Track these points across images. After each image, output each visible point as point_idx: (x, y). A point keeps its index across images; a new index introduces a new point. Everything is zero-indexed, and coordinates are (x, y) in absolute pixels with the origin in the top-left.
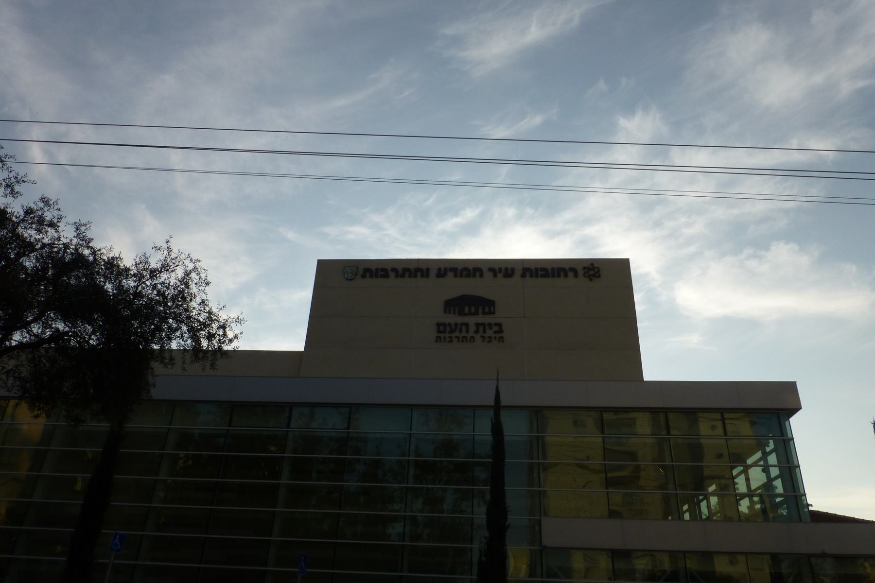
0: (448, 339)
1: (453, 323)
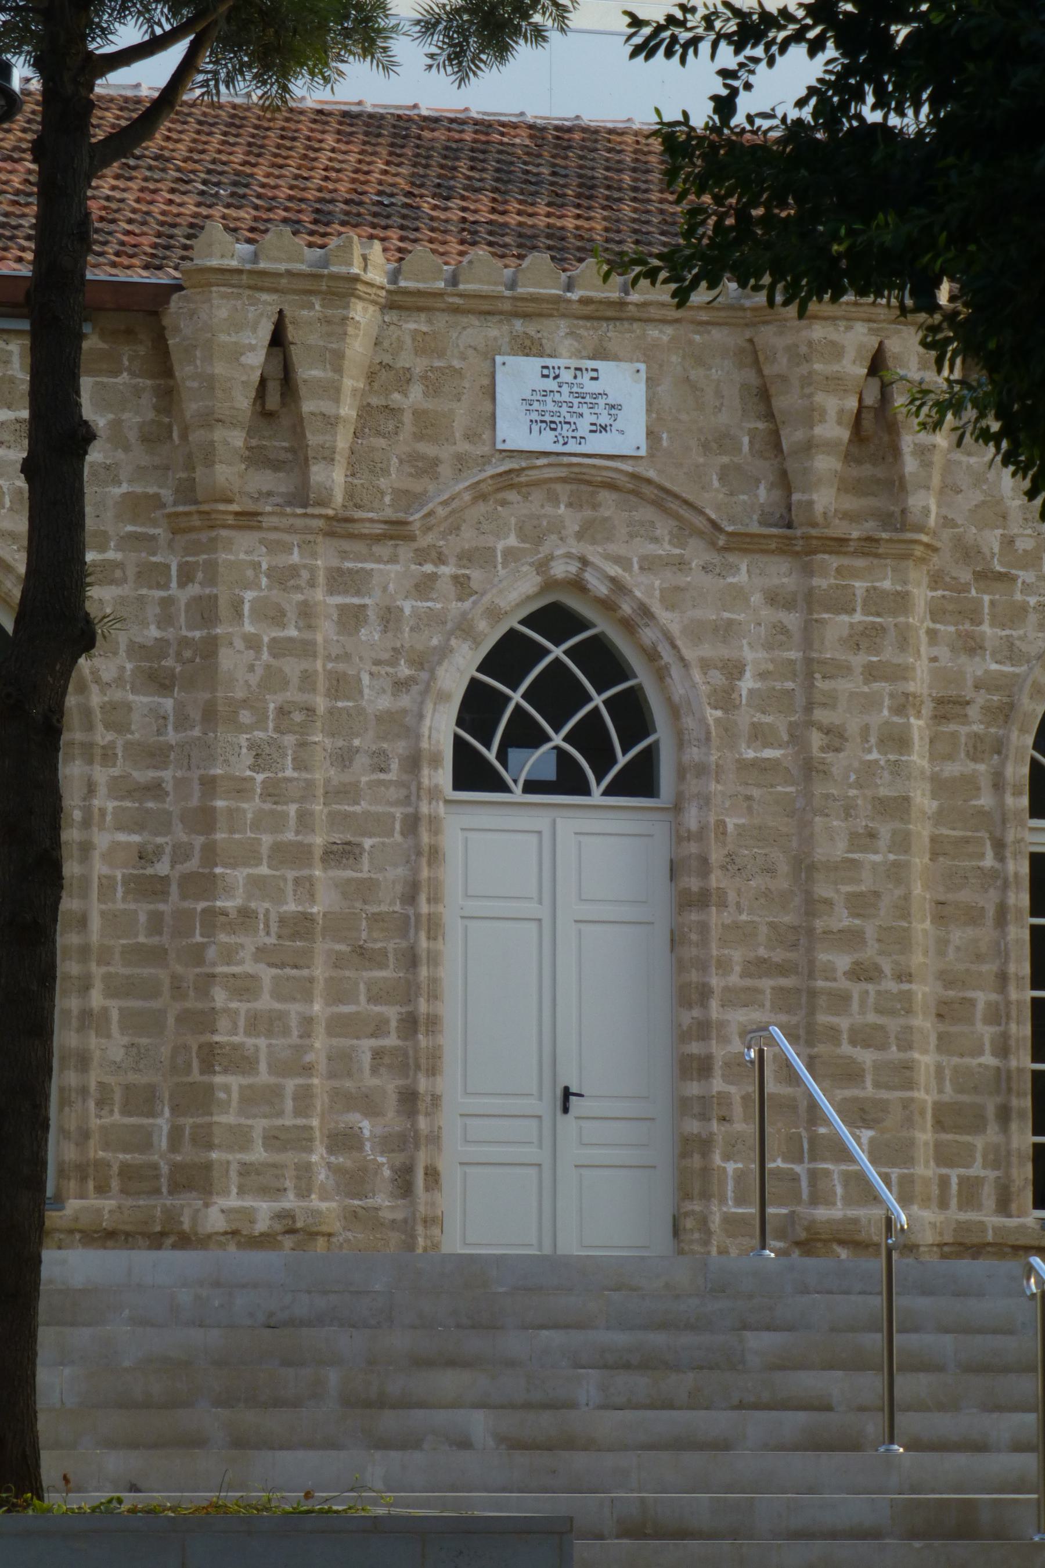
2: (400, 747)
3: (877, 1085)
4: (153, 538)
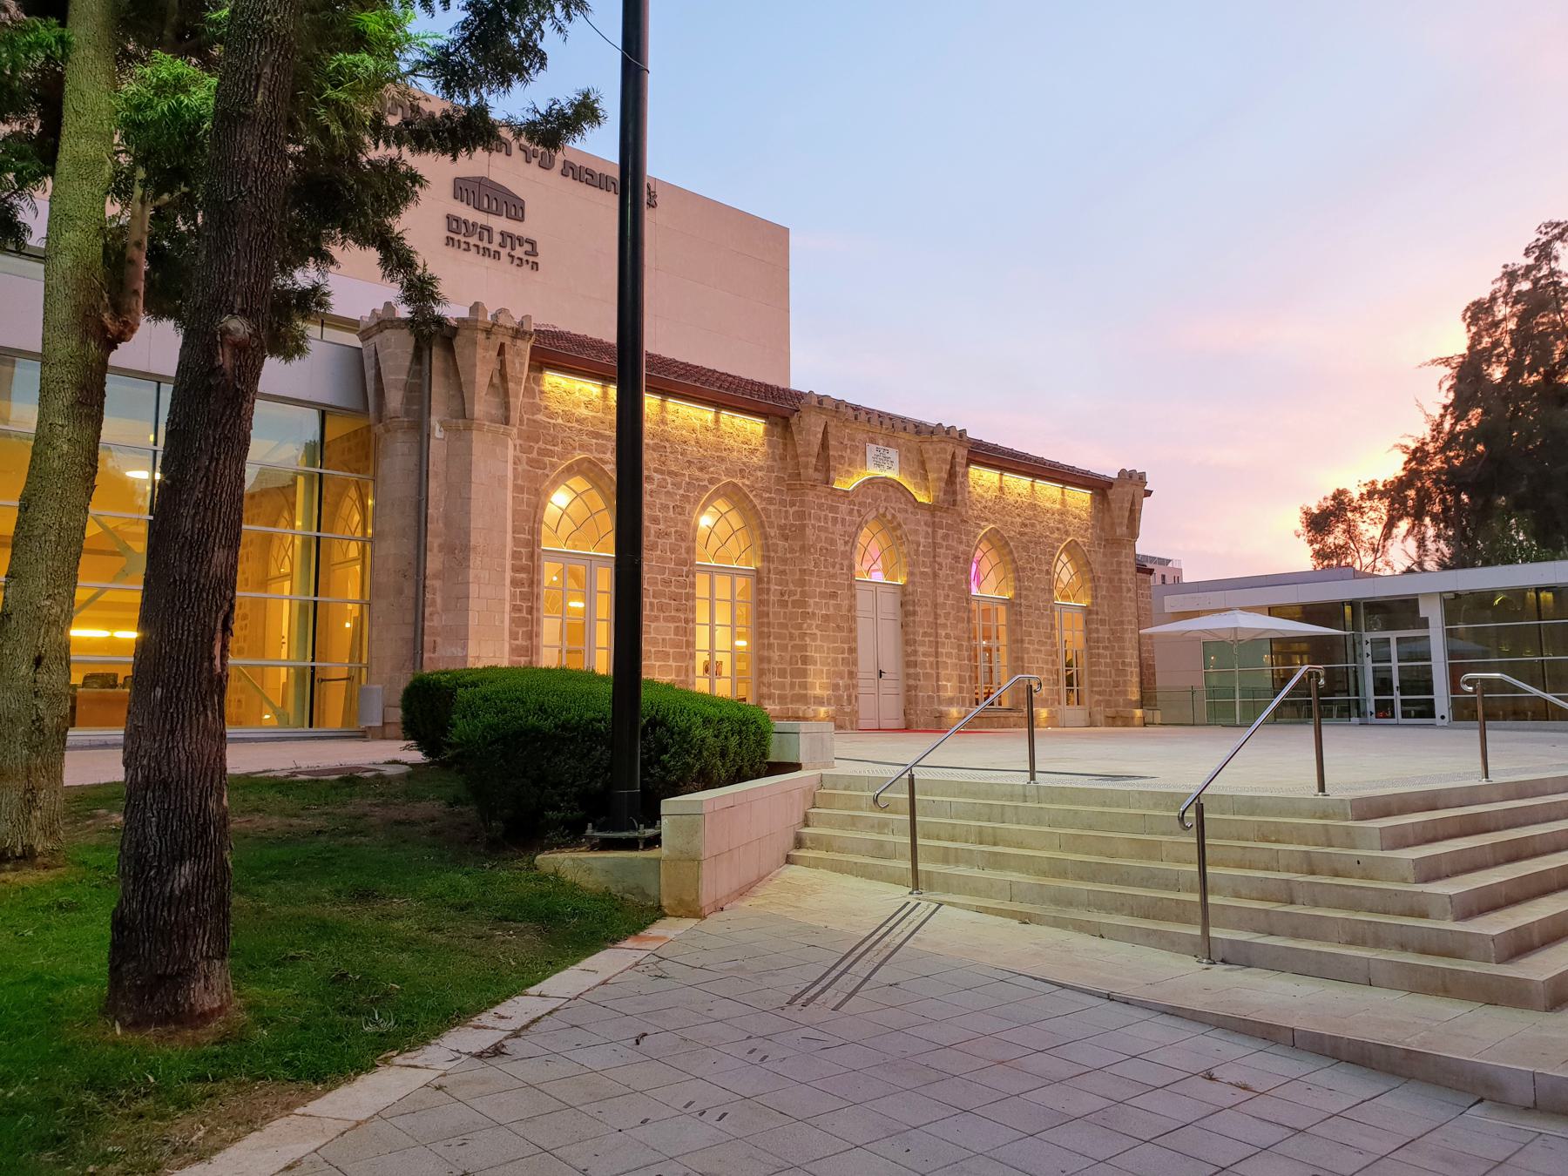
0: (463, 246)
2: (846, 563)
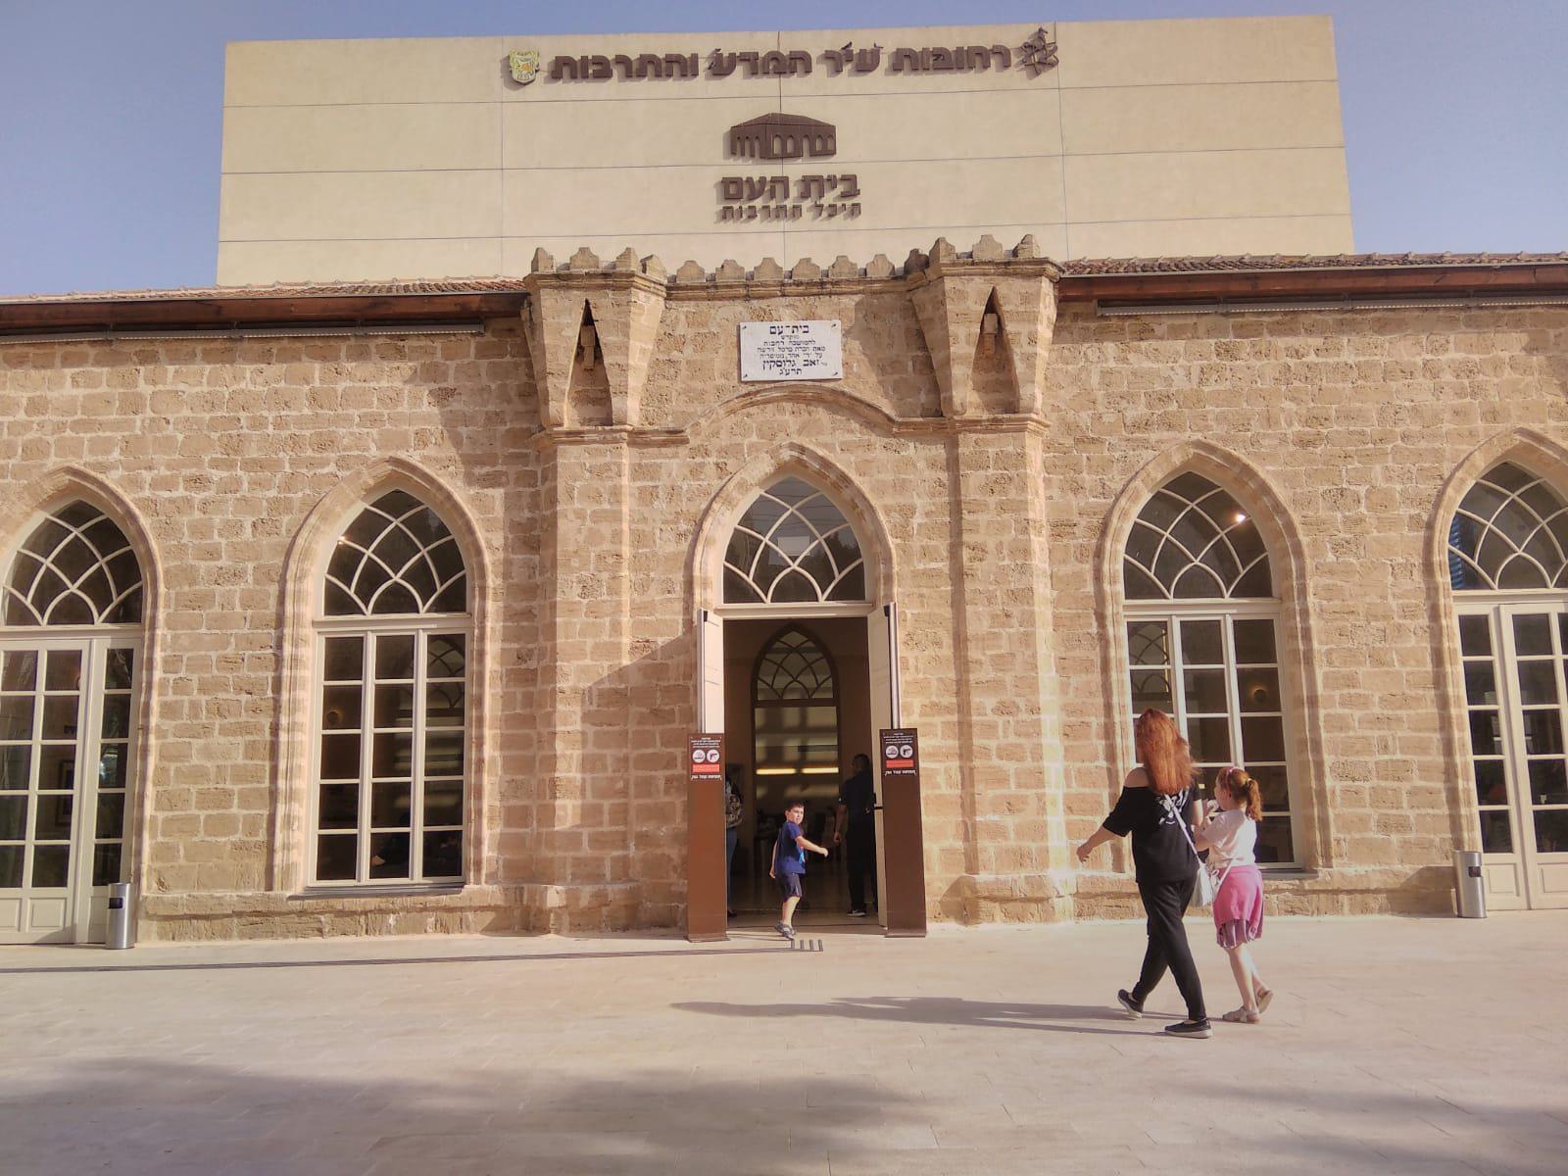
1: (756, 179)
3: (1019, 786)
4: (526, 455)
